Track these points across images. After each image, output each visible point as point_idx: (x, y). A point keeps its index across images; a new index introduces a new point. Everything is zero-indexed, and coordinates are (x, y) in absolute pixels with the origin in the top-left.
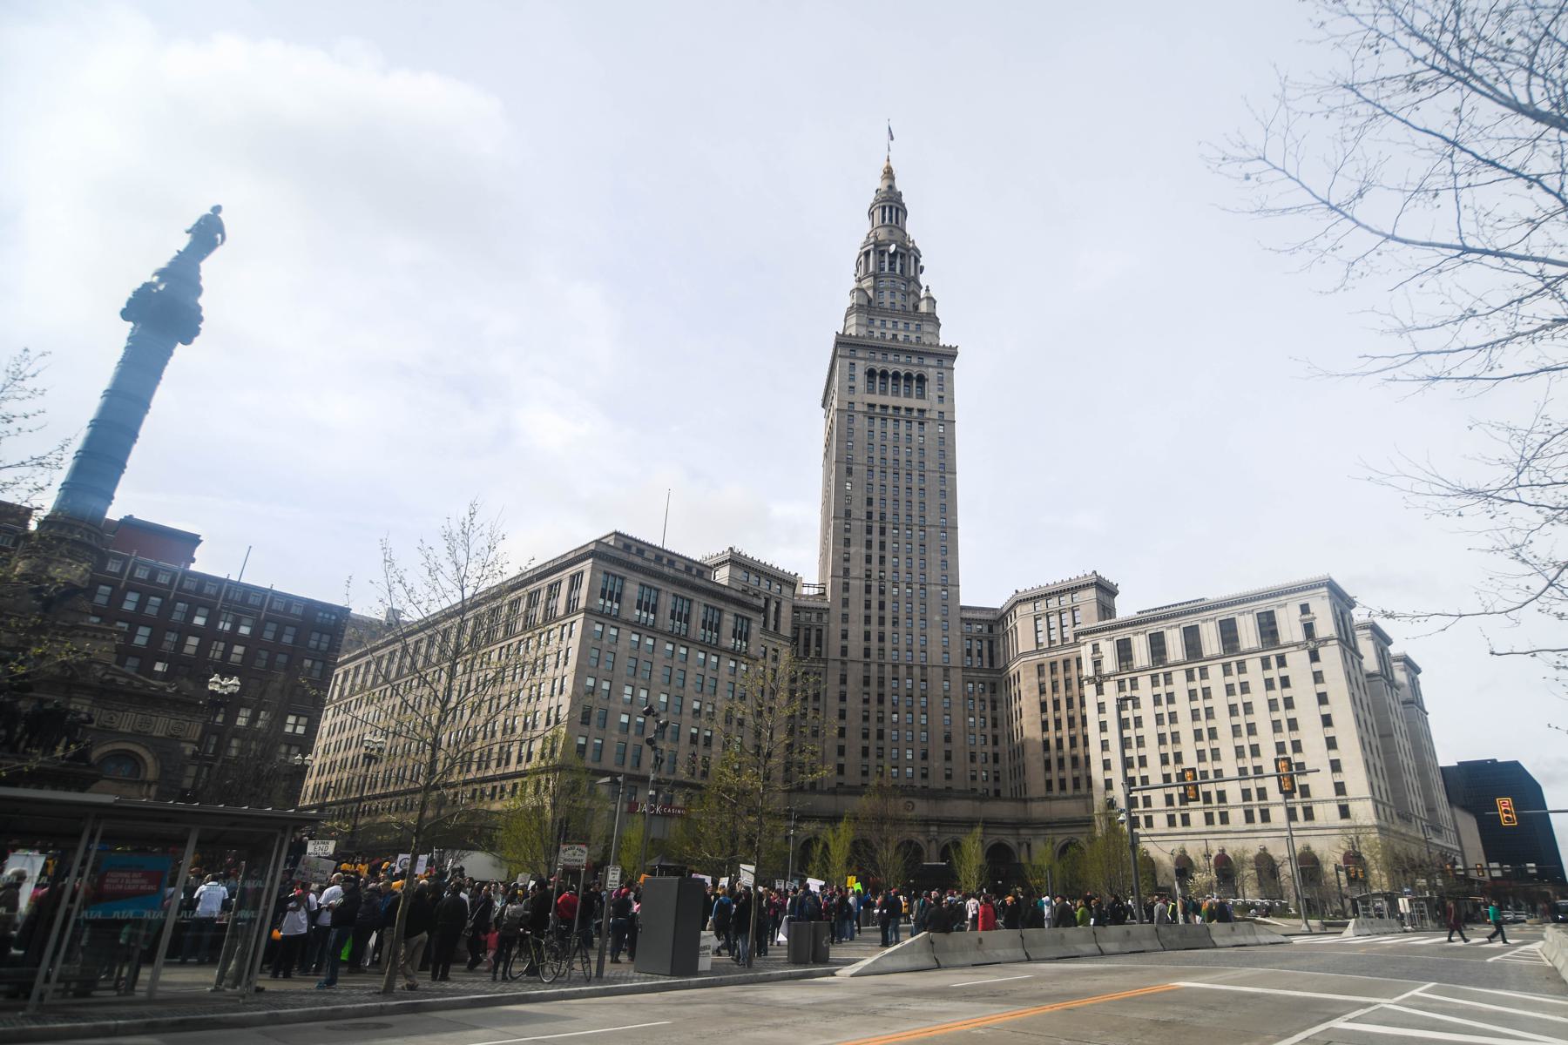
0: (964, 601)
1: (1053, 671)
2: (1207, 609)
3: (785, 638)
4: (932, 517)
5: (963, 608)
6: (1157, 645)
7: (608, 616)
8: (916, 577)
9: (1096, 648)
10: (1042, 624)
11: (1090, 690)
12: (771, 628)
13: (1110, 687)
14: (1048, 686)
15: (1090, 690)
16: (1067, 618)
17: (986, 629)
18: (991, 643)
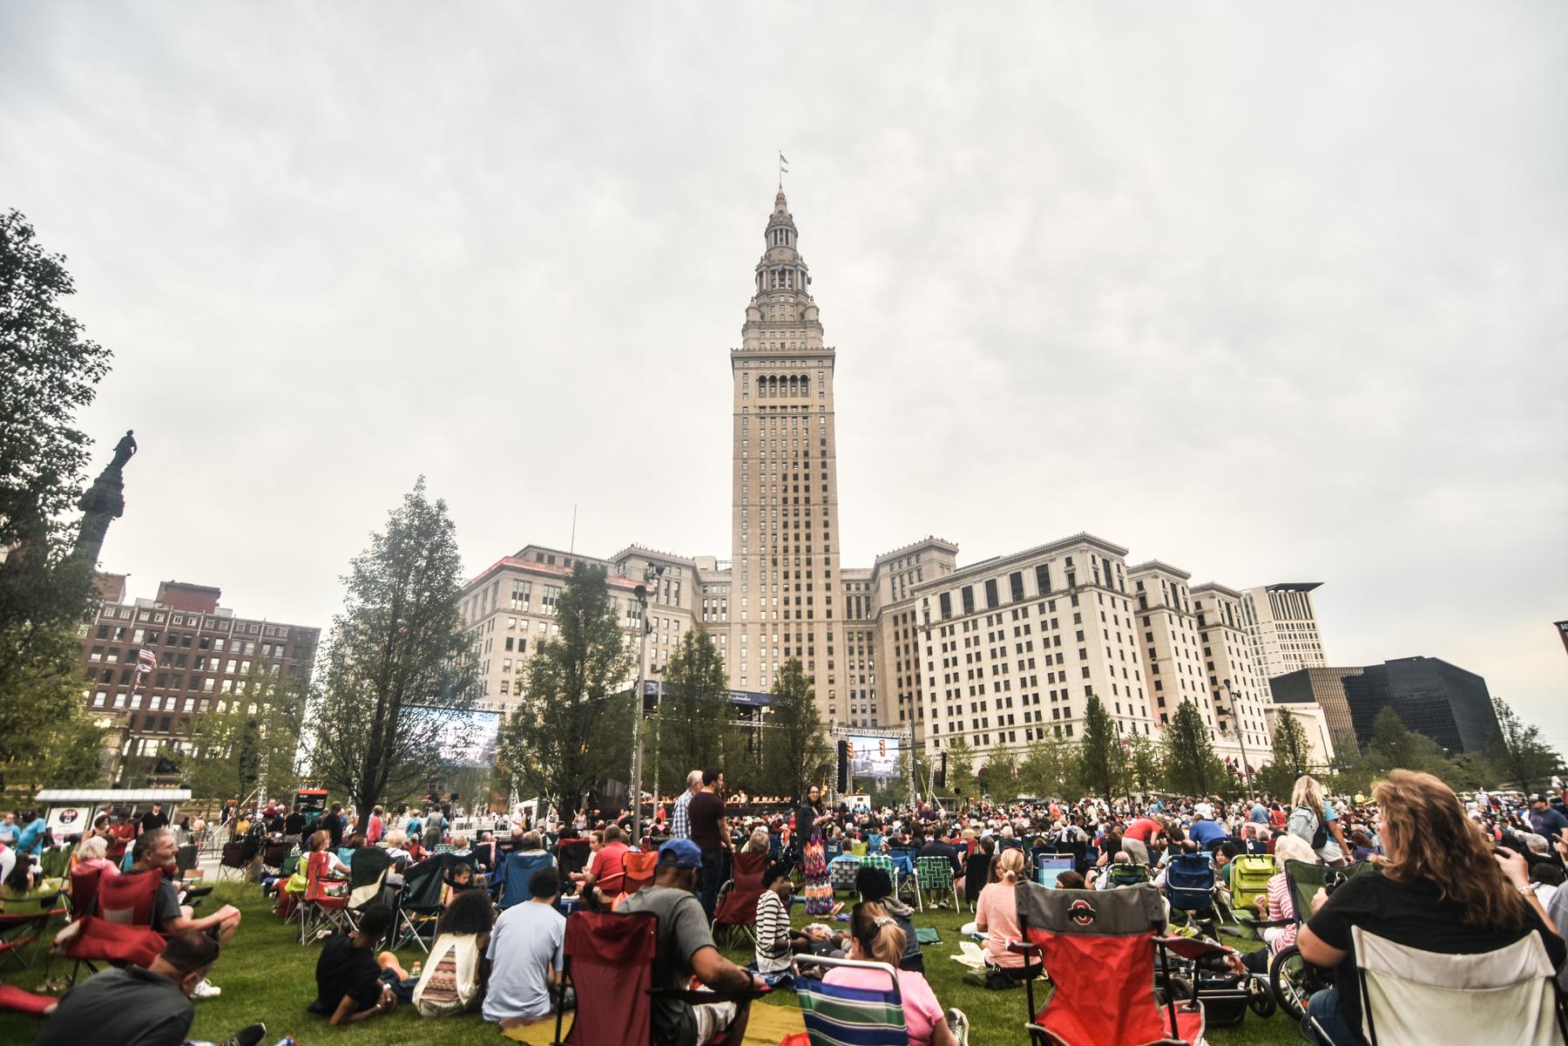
0: (843, 566)
1: (905, 621)
2: (995, 567)
3: (685, 611)
4: (816, 495)
5: (843, 571)
6: (968, 595)
7: (519, 613)
8: (803, 549)
9: (926, 601)
10: (897, 580)
11: (922, 636)
12: (673, 602)
13: (936, 633)
14: (901, 634)
15: (922, 636)
16: (915, 574)
17: (863, 587)
18: (867, 598)
